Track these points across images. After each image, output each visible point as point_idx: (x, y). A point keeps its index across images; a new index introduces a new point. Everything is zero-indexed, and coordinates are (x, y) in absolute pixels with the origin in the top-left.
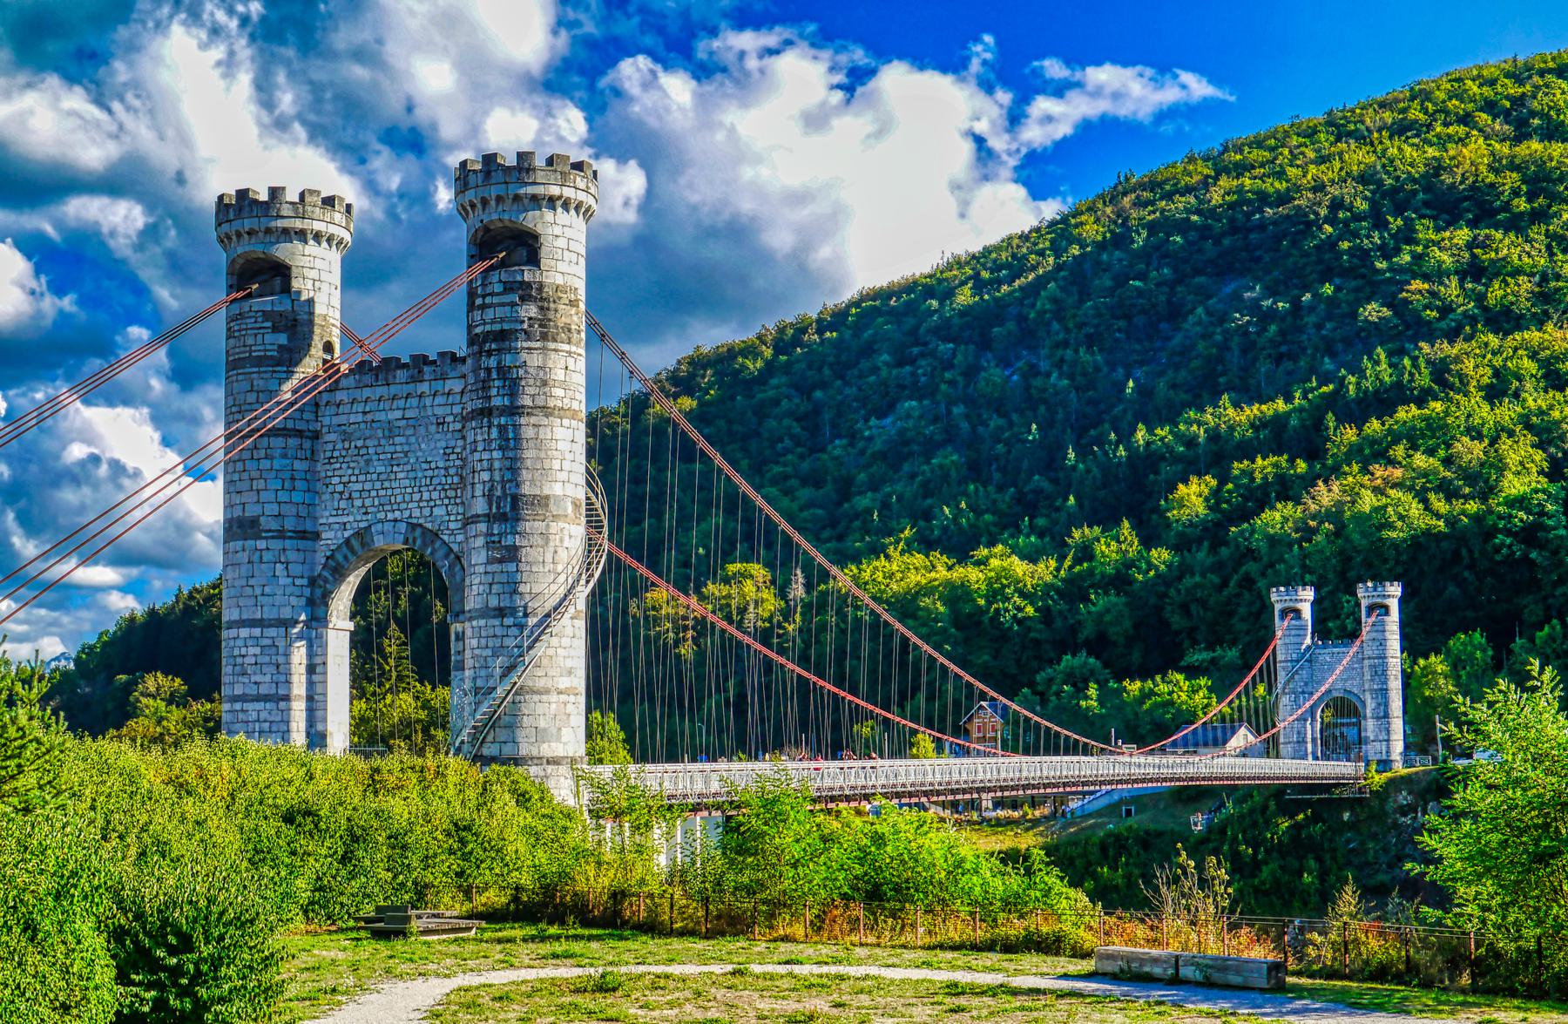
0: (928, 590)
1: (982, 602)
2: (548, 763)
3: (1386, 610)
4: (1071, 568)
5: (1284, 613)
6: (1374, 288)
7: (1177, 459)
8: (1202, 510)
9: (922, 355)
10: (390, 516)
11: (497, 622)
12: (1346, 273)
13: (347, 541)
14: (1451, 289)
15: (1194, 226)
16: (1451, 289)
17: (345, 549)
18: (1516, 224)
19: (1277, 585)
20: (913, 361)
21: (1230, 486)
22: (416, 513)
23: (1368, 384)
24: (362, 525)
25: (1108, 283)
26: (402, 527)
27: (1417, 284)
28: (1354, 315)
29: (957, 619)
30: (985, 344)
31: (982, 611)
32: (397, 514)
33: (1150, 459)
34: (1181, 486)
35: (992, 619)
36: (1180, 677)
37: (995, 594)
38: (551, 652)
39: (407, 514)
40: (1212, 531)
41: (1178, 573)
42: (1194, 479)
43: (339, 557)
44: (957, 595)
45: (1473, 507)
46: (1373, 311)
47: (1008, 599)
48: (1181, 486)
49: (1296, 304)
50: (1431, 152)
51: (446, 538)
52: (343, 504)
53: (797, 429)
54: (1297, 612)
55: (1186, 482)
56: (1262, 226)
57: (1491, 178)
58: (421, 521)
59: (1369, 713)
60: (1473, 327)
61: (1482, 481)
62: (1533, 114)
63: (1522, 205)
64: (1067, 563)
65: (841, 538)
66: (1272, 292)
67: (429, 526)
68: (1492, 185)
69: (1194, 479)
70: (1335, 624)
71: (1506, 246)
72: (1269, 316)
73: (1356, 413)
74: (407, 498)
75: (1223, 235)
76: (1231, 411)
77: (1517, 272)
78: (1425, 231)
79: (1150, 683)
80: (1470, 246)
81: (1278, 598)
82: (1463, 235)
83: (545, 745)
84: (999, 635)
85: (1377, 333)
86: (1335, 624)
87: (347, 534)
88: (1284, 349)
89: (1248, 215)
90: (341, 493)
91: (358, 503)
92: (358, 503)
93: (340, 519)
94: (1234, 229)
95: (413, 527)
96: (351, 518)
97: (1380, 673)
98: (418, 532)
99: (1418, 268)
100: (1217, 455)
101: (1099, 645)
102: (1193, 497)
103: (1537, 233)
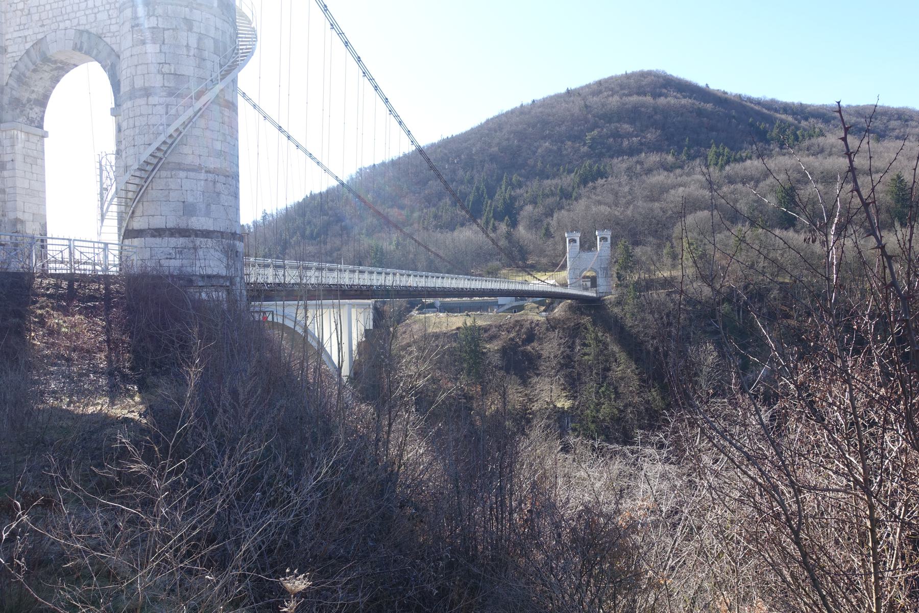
2: (196, 236)
10: (62, 26)
11: (142, 101)
13: (27, 52)
17: (26, 59)
22: (83, 21)
24: (40, 36)
26: (71, 33)
32: (68, 23)
38: (197, 132)
39: (75, 22)
43: (22, 67)
51: (108, 40)
52: (24, 20)
58: (87, 27)
67: (93, 31)
70: (587, 245)
74: (76, 8)
83: (194, 219)
87: (28, 46)
90: (22, 10)
91: (36, 17)
92: (36, 17)
93: (21, 34)
95: (81, 32)
96: (30, 32)
98: (85, 36)
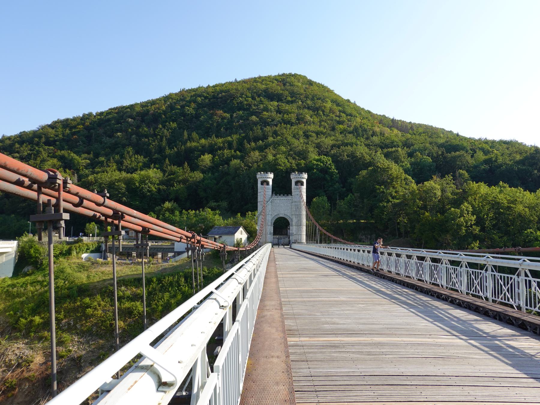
0: (119, 181)
1: (137, 184)
3: (302, 184)
4: (167, 176)
5: (262, 183)
6: (253, 113)
7: (199, 151)
8: (209, 163)
9: (123, 122)
12: (244, 110)
14: (274, 114)
15: (204, 96)
16: (274, 114)
18: (288, 102)
19: (260, 172)
20: (121, 124)
21: (217, 157)
23: (255, 134)
25: (179, 107)
27: (265, 113)
28: (248, 119)
29: (128, 189)
30: (143, 121)
31: (137, 188)
33: (191, 150)
34: (202, 156)
35: (140, 190)
36: (209, 210)
37: (142, 181)
40: (213, 168)
41: (203, 180)
42: (206, 154)
44: (129, 183)
45: (303, 162)
46: (254, 118)
47: (145, 184)
48: (202, 156)
49: (232, 116)
50: (264, 86)
53: (84, 139)
54: (268, 183)
55: (204, 155)
56: (221, 98)
57: (281, 92)
59: (294, 223)
60: (281, 124)
61: (303, 155)
62: (286, 82)
63: (289, 99)
64: (167, 174)
65: (93, 168)
66: (225, 112)
68: (282, 94)
69: (206, 154)
70: (282, 187)
71: (287, 107)
72: (223, 118)
73: (256, 139)
75: (211, 99)
76: (215, 139)
77: (290, 113)
78: (266, 101)
79: (198, 212)
80: (278, 106)
81: (260, 177)
82: (276, 103)
84: (143, 196)
85: (255, 124)
86: (282, 187)
88: (228, 126)
89: (218, 95)
94: (214, 97)
97: (299, 208)
99: (266, 109)
100: (212, 150)
101: (176, 200)
102: (207, 158)
103: (295, 105)
